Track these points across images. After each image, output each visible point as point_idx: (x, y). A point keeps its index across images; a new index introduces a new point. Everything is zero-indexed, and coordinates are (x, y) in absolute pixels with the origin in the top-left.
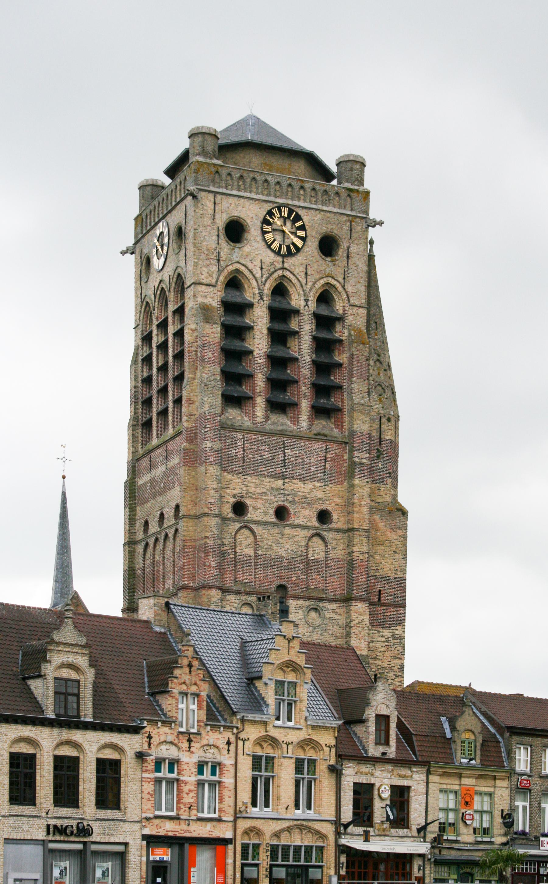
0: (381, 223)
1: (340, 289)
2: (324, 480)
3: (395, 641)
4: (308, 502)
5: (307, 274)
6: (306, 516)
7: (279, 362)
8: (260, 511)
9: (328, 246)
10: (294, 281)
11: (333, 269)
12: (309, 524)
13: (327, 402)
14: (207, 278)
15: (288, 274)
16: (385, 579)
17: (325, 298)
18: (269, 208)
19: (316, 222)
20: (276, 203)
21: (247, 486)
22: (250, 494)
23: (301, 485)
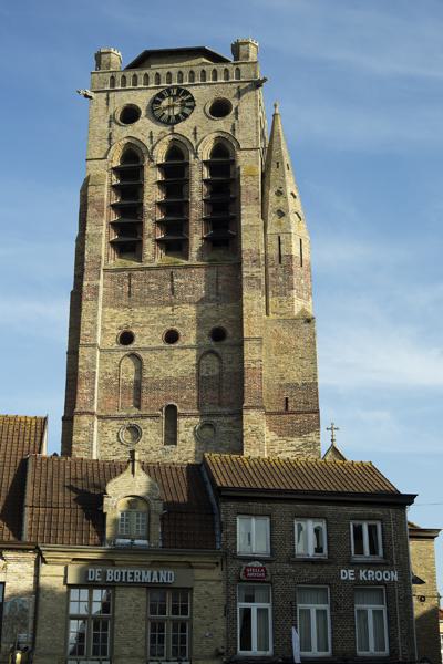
0: (265, 80)
5: (202, 134)
7: (175, 207)
11: (222, 125)
13: (224, 234)
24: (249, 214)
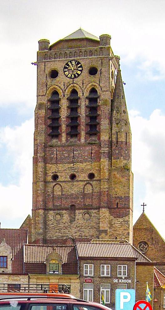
1: (98, 86)
2: (91, 161)
3: (125, 223)
4: (82, 171)
6: (83, 176)
7: (74, 119)
8: (64, 177)
9: (93, 71)
10: (78, 87)
12: (84, 179)
14: (42, 93)
15: (75, 85)
16: (120, 198)
17: (93, 91)
18: (67, 62)
19: (86, 62)
20: (69, 60)
21: (58, 168)
22: (59, 171)
23: (81, 164)
24: (104, 124)
